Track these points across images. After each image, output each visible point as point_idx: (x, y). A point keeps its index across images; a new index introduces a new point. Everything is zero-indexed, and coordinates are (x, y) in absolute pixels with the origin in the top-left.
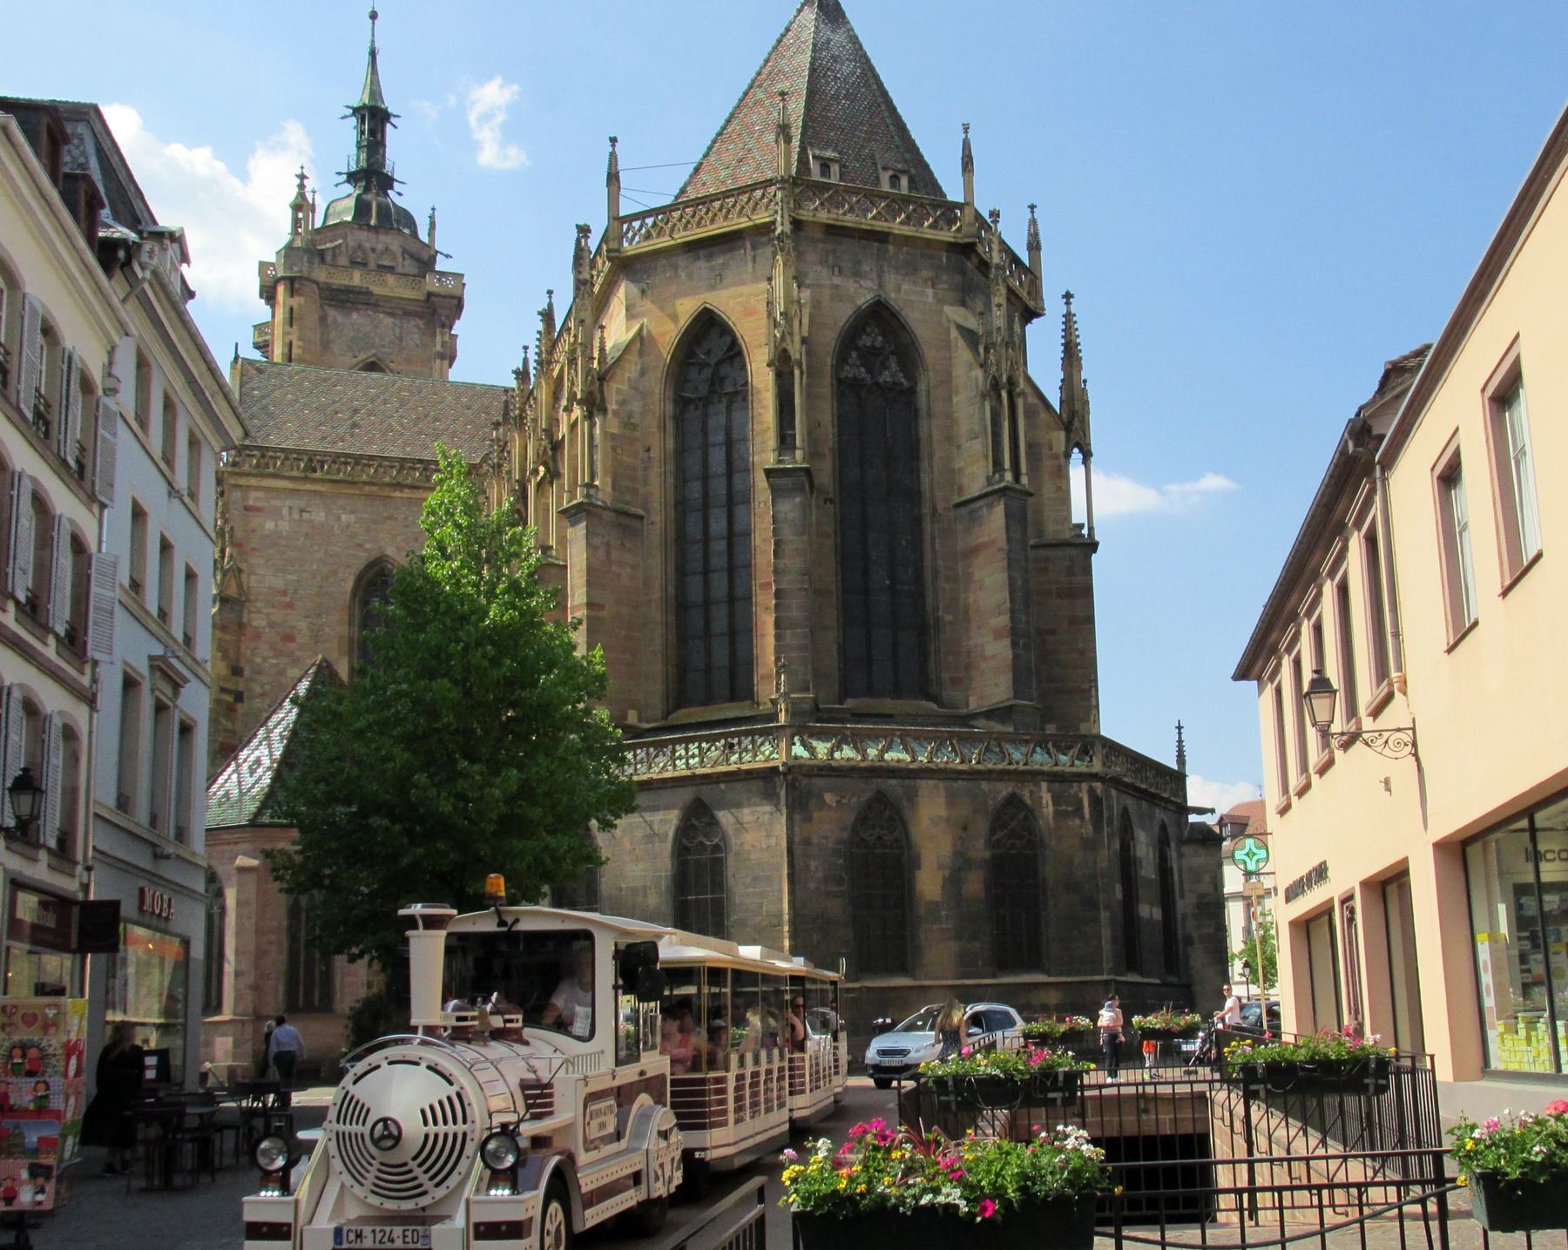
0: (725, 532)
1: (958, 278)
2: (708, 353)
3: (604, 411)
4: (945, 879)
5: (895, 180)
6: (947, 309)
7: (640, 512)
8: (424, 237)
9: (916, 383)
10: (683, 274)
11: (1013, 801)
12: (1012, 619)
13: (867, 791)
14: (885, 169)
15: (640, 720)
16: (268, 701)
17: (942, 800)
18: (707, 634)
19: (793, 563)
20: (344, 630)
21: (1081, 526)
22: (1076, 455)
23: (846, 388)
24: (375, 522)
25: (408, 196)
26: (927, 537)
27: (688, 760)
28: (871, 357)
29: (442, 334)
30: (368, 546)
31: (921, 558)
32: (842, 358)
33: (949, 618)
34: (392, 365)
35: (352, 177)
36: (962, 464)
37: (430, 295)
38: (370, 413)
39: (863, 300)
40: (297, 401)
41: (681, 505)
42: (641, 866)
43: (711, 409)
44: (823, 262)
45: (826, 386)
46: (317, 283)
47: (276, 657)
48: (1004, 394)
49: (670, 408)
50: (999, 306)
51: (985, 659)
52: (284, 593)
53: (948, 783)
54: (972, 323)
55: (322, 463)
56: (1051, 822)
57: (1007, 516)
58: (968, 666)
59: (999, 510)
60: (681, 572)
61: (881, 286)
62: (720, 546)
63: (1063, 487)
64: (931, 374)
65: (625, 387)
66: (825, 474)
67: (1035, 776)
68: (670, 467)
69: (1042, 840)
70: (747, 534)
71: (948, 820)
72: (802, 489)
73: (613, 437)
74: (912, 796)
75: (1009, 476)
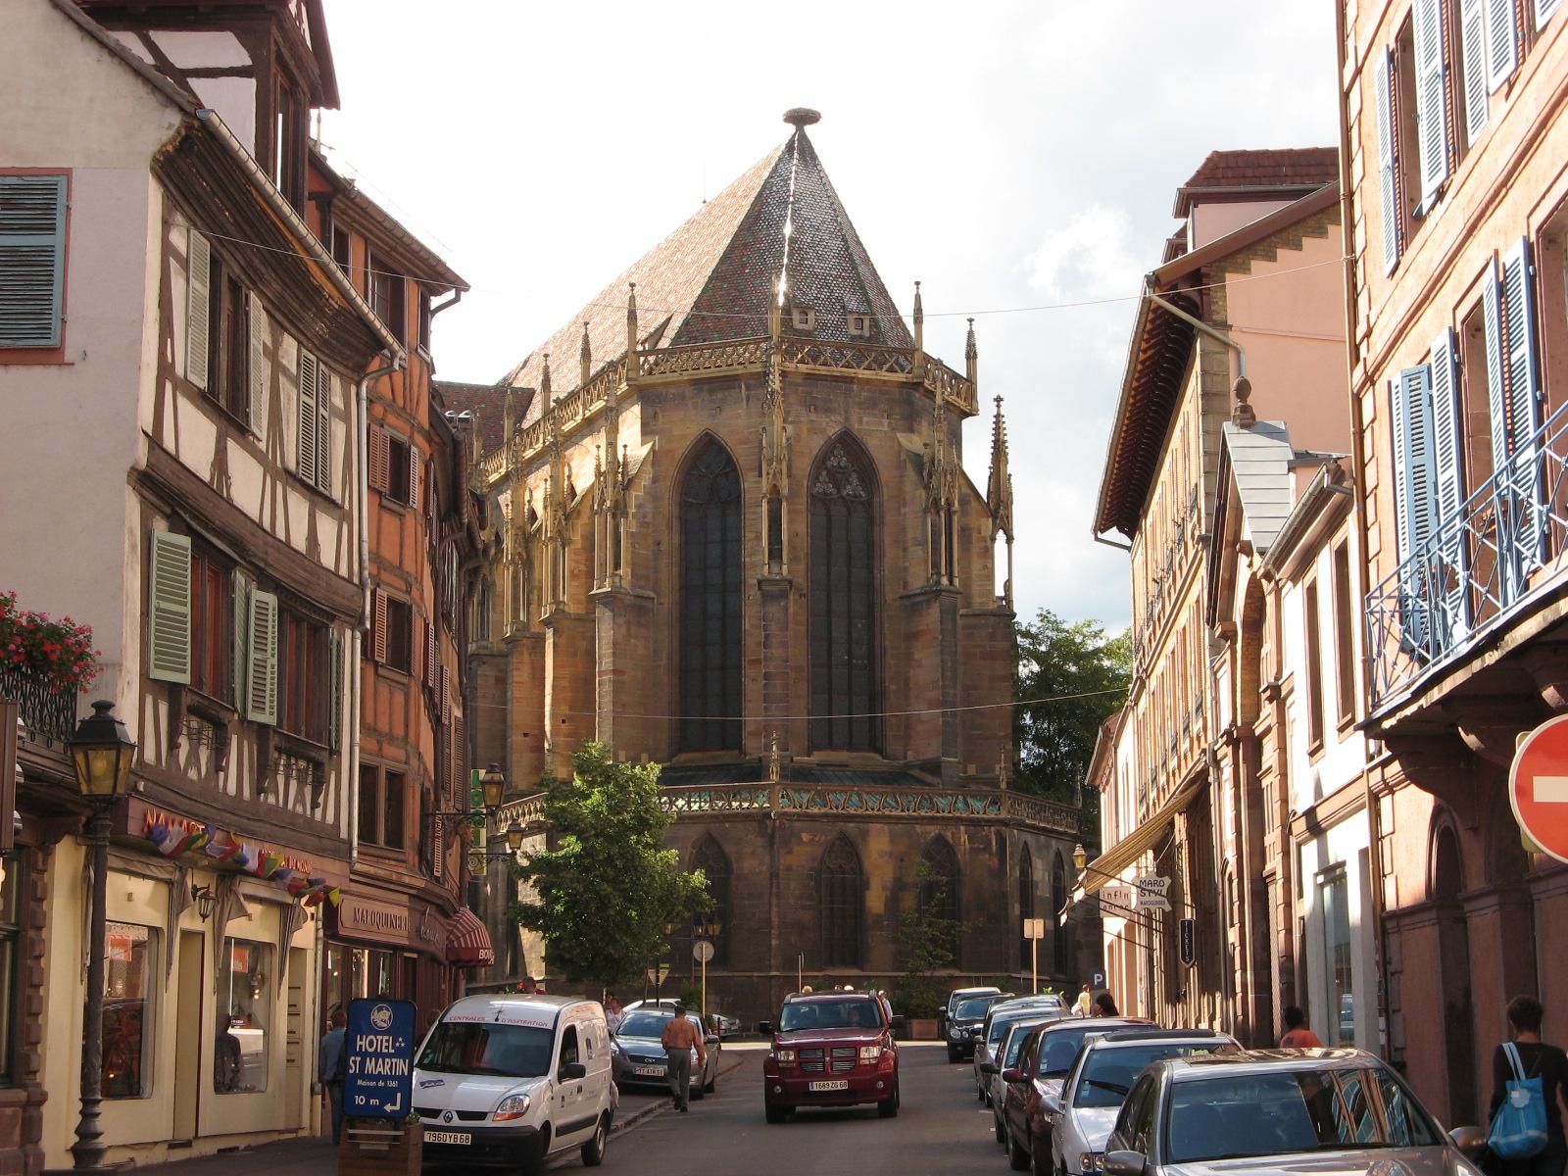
3: (625, 514)
4: (886, 897)
7: (652, 594)
9: (872, 497)
10: (690, 403)
11: (940, 839)
17: (888, 839)
22: (1001, 536)
23: (817, 500)
28: (837, 477)
32: (815, 478)
33: (893, 687)
36: (907, 564)
39: (833, 431)
41: (685, 589)
45: (802, 503)
49: (675, 511)
50: (939, 441)
53: (892, 826)
56: (967, 857)
57: (941, 611)
61: (847, 419)
63: (990, 566)
64: (885, 490)
66: (801, 579)
68: (676, 559)
69: (959, 870)
70: (739, 617)
71: (891, 854)
74: (865, 835)
75: (945, 581)
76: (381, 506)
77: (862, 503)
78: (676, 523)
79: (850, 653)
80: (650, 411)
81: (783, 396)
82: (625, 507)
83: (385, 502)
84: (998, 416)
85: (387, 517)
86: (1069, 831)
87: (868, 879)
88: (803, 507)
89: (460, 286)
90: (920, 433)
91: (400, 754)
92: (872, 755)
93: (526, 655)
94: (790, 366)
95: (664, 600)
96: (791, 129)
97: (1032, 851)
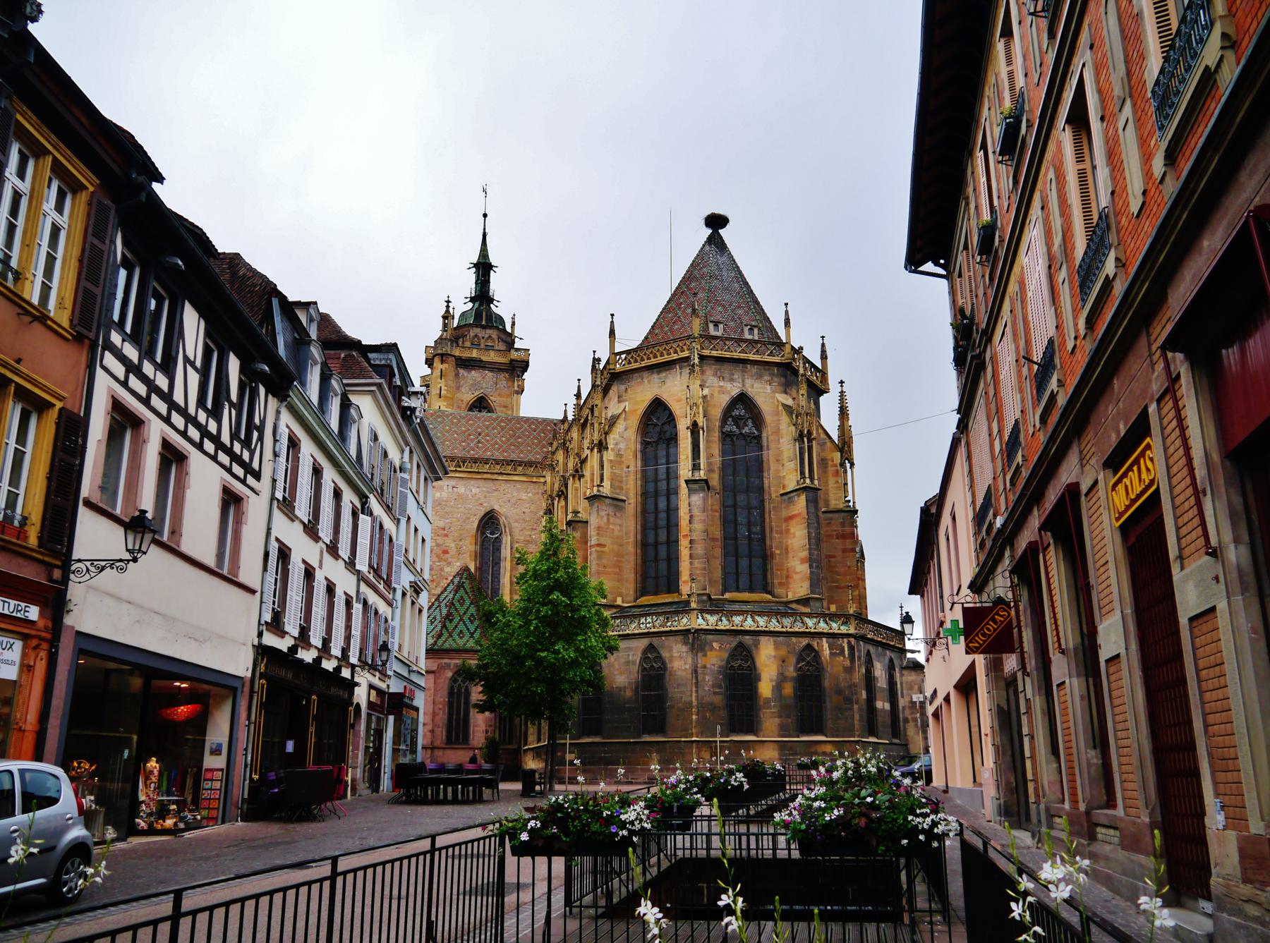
0: (665, 508)
1: (783, 379)
2: (658, 419)
5: (751, 330)
6: (777, 395)
8: (509, 329)
11: (809, 647)
12: (810, 554)
13: (734, 641)
14: (746, 325)
15: (623, 602)
16: (435, 584)
17: (772, 647)
18: (656, 559)
19: (698, 526)
20: (472, 548)
23: (726, 437)
24: (489, 492)
25: (501, 308)
26: (767, 511)
27: (648, 624)
28: (737, 420)
29: (518, 381)
30: (485, 505)
31: (764, 522)
32: (724, 421)
33: (778, 552)
34: (491, 398)
35: (472, 300)
37: (512, 360)
38: (487, 435)
40: (450, 430)
41: (645, 494)
42: (623, 677)
43: (659, 446)
44: (715, 374)
45: (716, 435)
46: (455, 356)
47: (439, 561)
48: (805, 440)
49: (639, 447)
50: (803, 395)
51: (797, 573)
52: (444, 529)
53: (775, 638)
54: (790, 402)
55: (464, 462)
56: (828, 658)
58: (788, 577)
59: (803, 498)
60: (644, 528)
61: (743, 385)
62: (663, 515)
64: (769, 429)
66: (715, 481)
67: (820, 635)
68: (639, 476)
69: (823, 668)
70: (677, 509)
71: (775, 657)
72: (704, 490)
73: (611, 461)
74: (757, 644)
75: (808, 481)
77: (754, 437)
79: (749, 531)
80: (623, 387)
81: (700, 367)
82: (607, 444)
84: (842, 393)
87: (760, 674)
88: (716, 439)
90: (790, 395)
92: (765, 595)
94: (706, 352)
95: (632, 501)
96: (709, 231)
97: (873, 656)
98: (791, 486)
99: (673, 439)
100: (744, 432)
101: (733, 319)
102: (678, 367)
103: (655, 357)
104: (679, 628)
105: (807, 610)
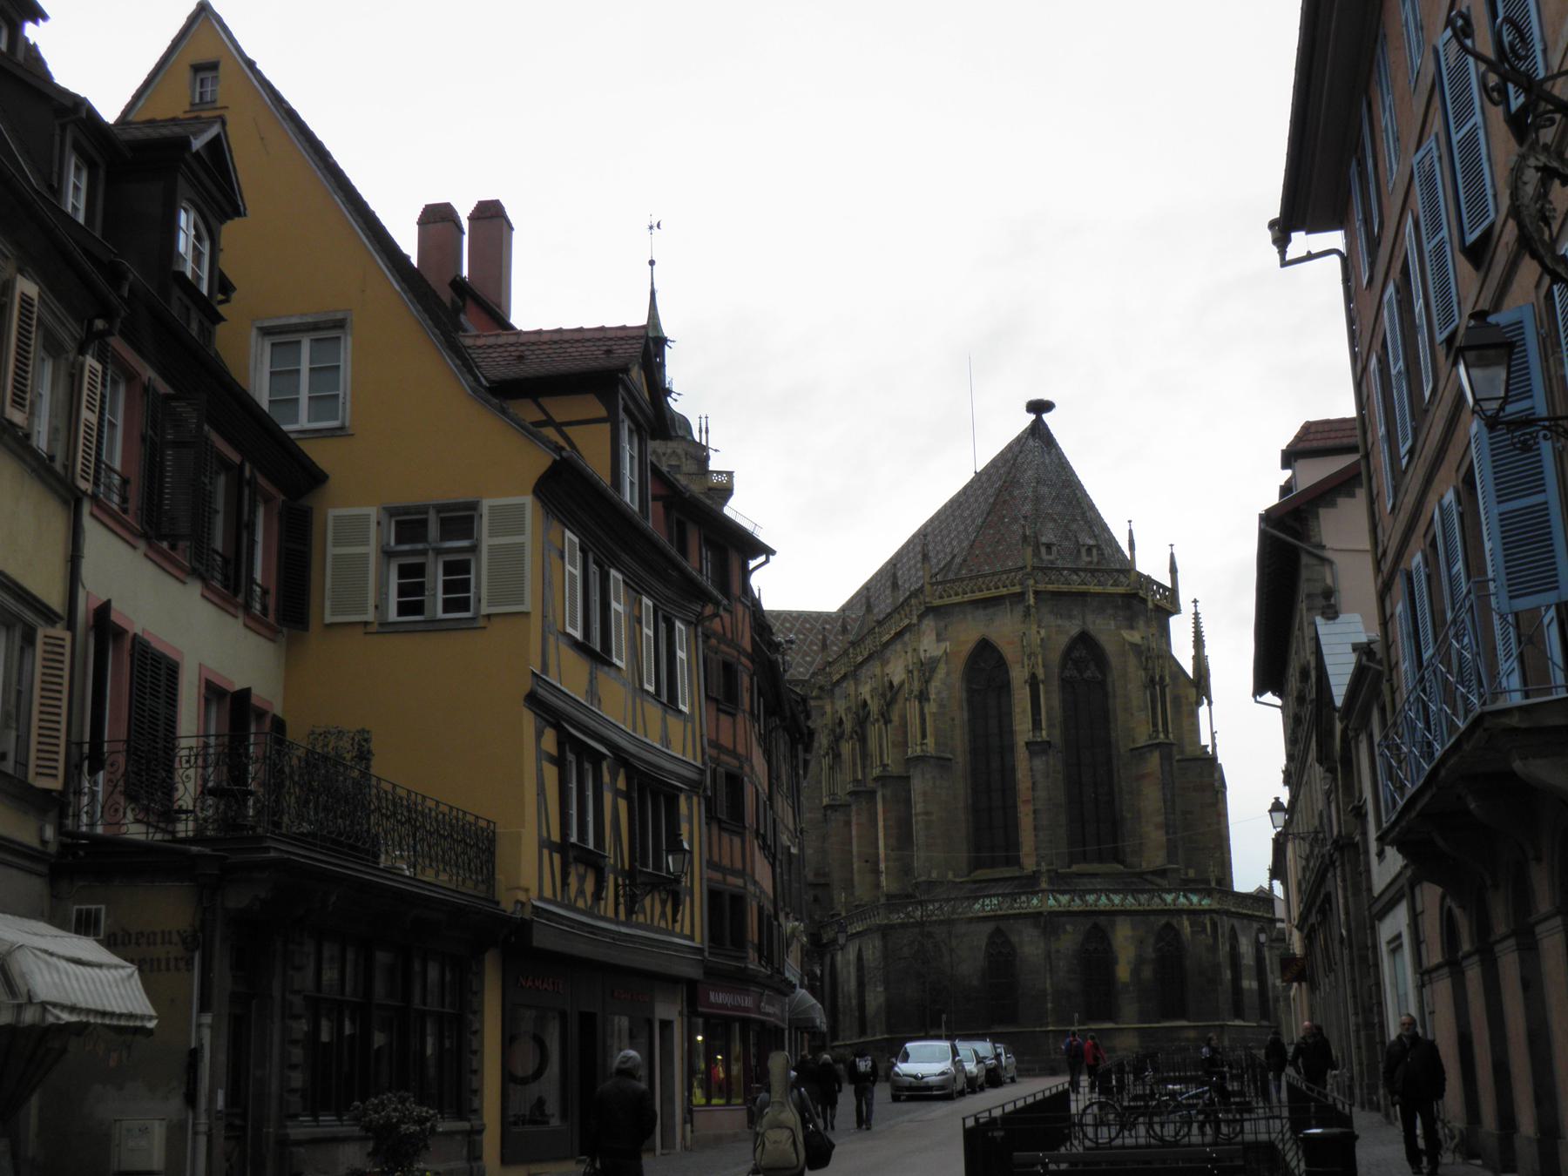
3: (928, 700)
7: (950, 756)
11: (1168, 925)
12: (1166, 818)
15: (955, 876)
21: (1207, 746)
23: (1067, 684)
32: (1063, 666)
33: (1129, 816)
37: (710, 489)
45: (1055, 683)
48: (1158, 688)
49: (964, 695)
57: (1161, 758)
59: (1156, 754)
61: (1084, 623)
65: (938, 684)
66: (1057, 738)
67: (1180, 912)
70: (1013, 769)
75: (1162, 736)
76: (719, 710)
78: (965, 705)
80: (942, 624)
82: (928, 693)
83: (721, 706)
84: (1196, 615)
85: (723, 717)
86: (1265, 915)
89: (768, 552)
91: (740, 882)
93: (864, 803)
94: (1041, 587)
96: (1033, 417)
97: (1238, 932)
98: (1142, 740)
99: (1005, 687)
100: (1085, 676)
101: (1067, 538)
102: (1008, 604)
103: (981, 590)
104: (1030, 910)
105: (1164, 883)
